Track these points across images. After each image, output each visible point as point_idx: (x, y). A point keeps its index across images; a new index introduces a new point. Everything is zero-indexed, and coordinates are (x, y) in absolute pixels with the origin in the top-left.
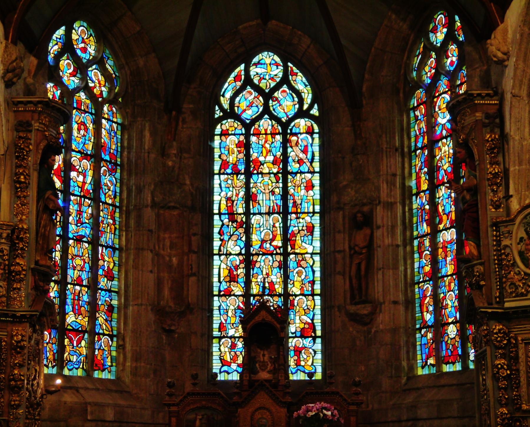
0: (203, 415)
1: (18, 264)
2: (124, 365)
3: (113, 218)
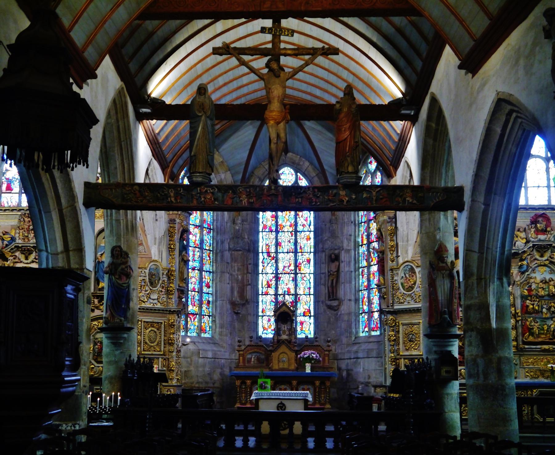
0: (255, 356)
1: (171, 287)
2: (215, 330)
3: (209, 257)
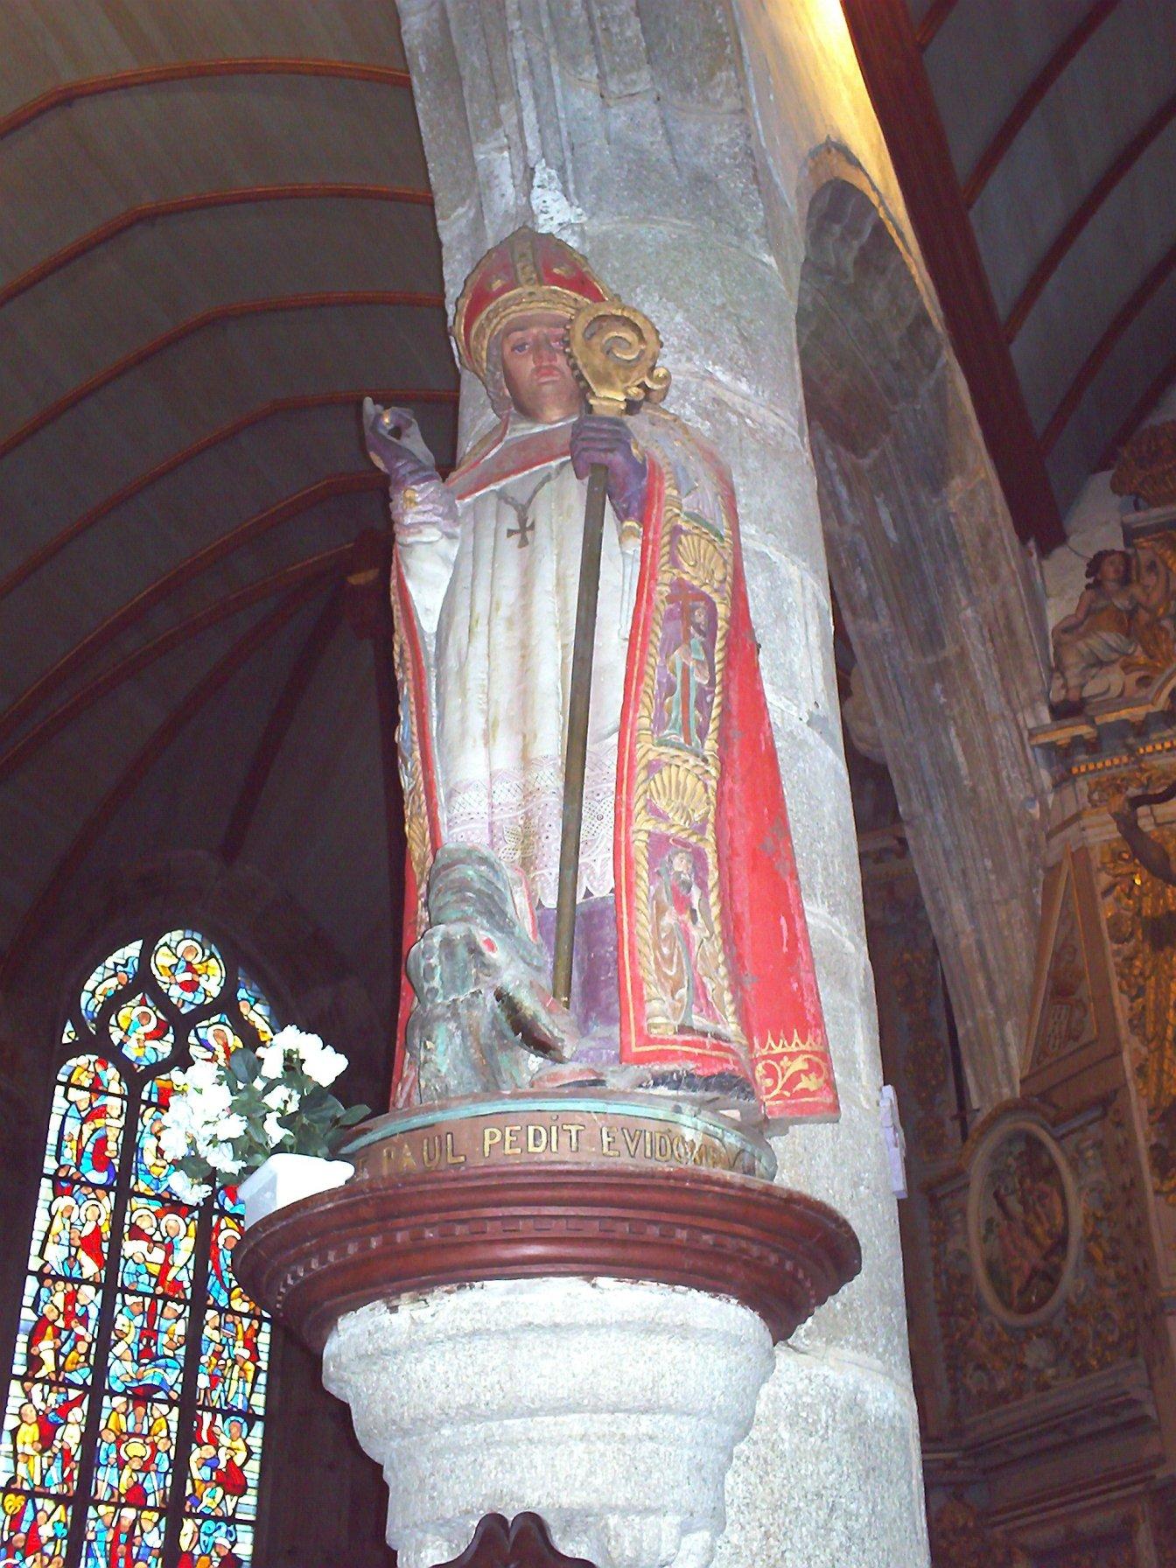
3: (252, 1347)
